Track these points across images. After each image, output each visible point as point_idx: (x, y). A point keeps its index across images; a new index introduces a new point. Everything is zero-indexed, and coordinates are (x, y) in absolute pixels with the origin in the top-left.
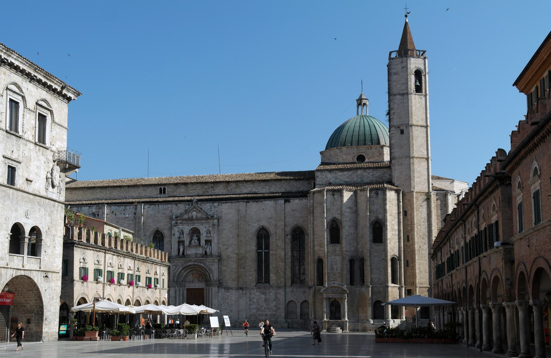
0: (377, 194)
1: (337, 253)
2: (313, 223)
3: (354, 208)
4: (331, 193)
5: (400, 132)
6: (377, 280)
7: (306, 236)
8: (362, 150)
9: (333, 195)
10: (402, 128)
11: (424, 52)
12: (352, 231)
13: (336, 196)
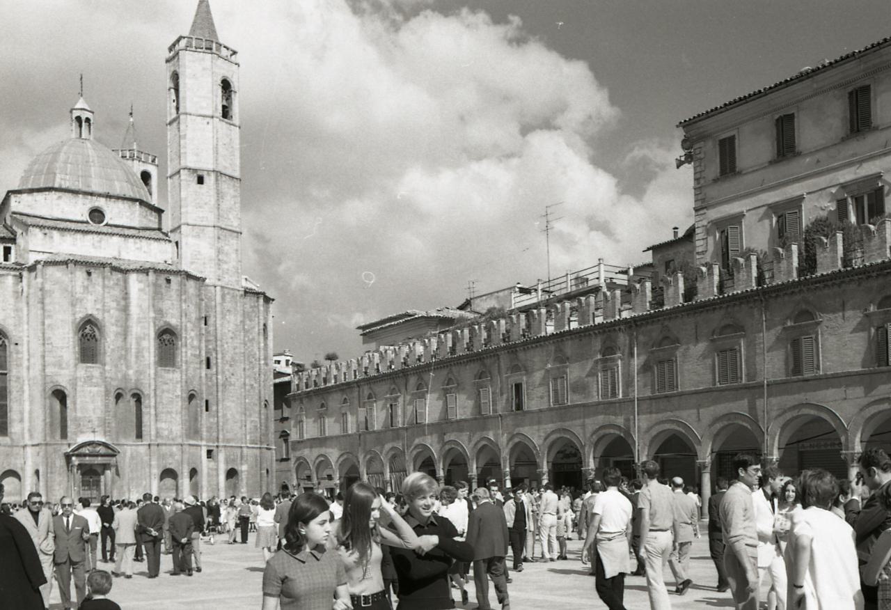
0: (168, 281)
1: (94, 380)
2: (43, 324)
3: (123, 303)
4: (84, 269)
5: (196, 179)
6: (166, 433)
7: (11, 348)
8: (101, 203)
9: (89, 274)
10: (200, 173)
11: (235, 53)
12: (119, 343)
13: (94, 275)
